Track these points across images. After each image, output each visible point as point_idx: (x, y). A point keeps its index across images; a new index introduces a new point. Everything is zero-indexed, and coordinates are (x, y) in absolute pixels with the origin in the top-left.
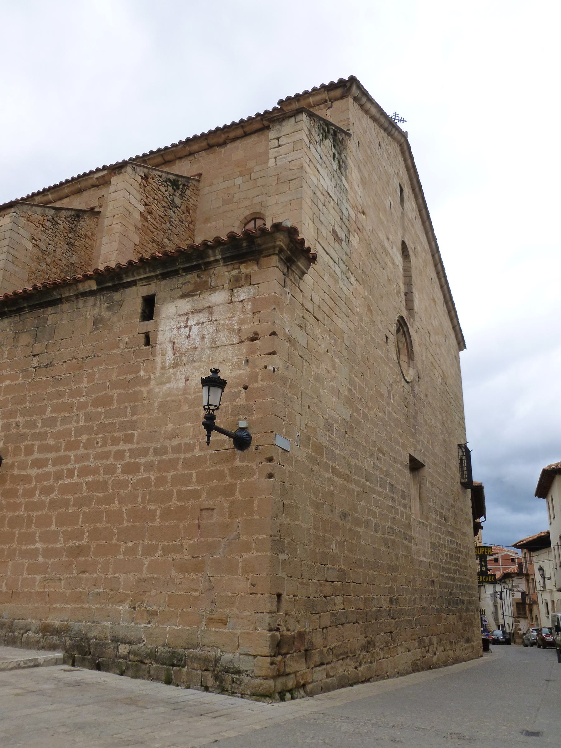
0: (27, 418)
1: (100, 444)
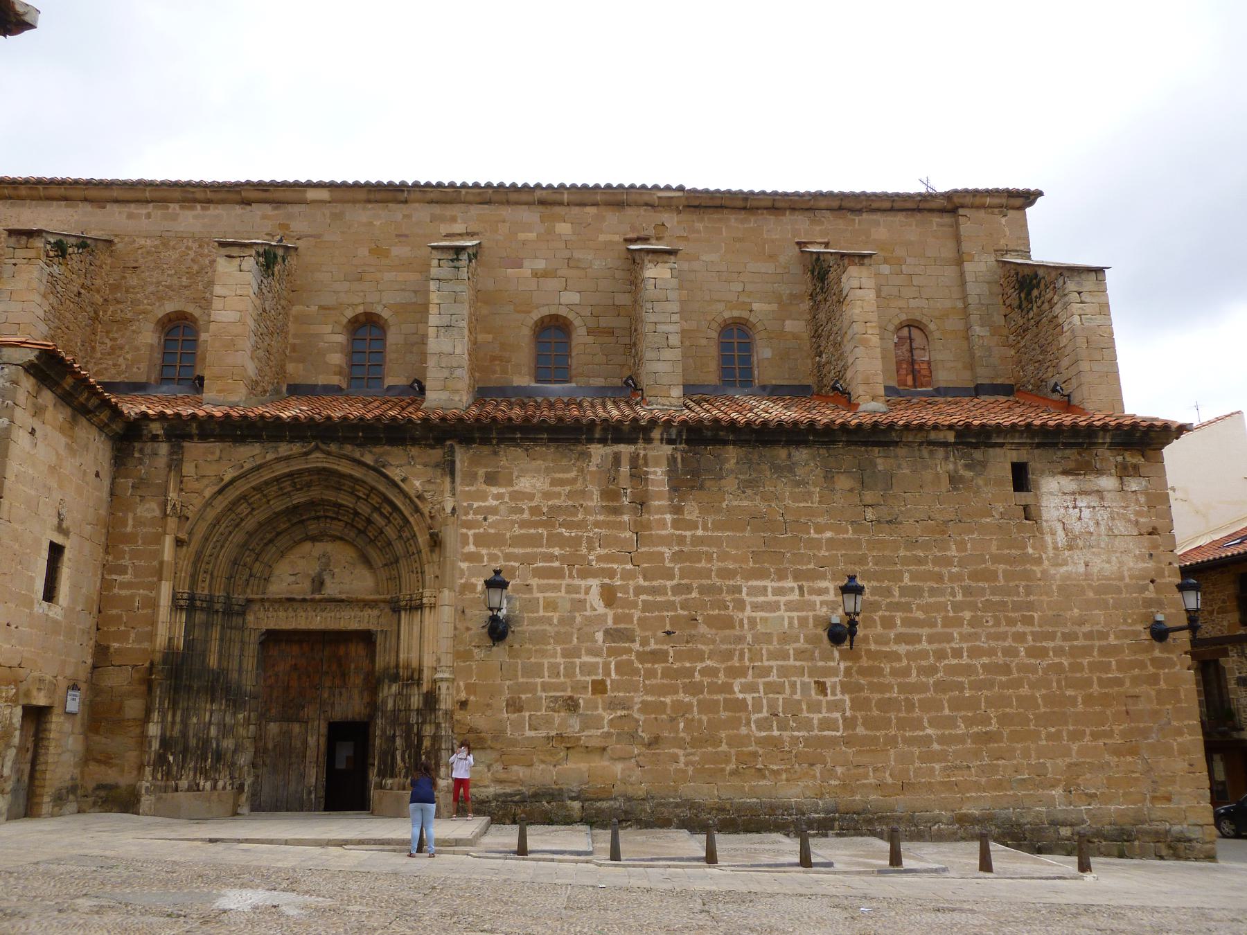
0: (875, 584)
1: (990, 624)
